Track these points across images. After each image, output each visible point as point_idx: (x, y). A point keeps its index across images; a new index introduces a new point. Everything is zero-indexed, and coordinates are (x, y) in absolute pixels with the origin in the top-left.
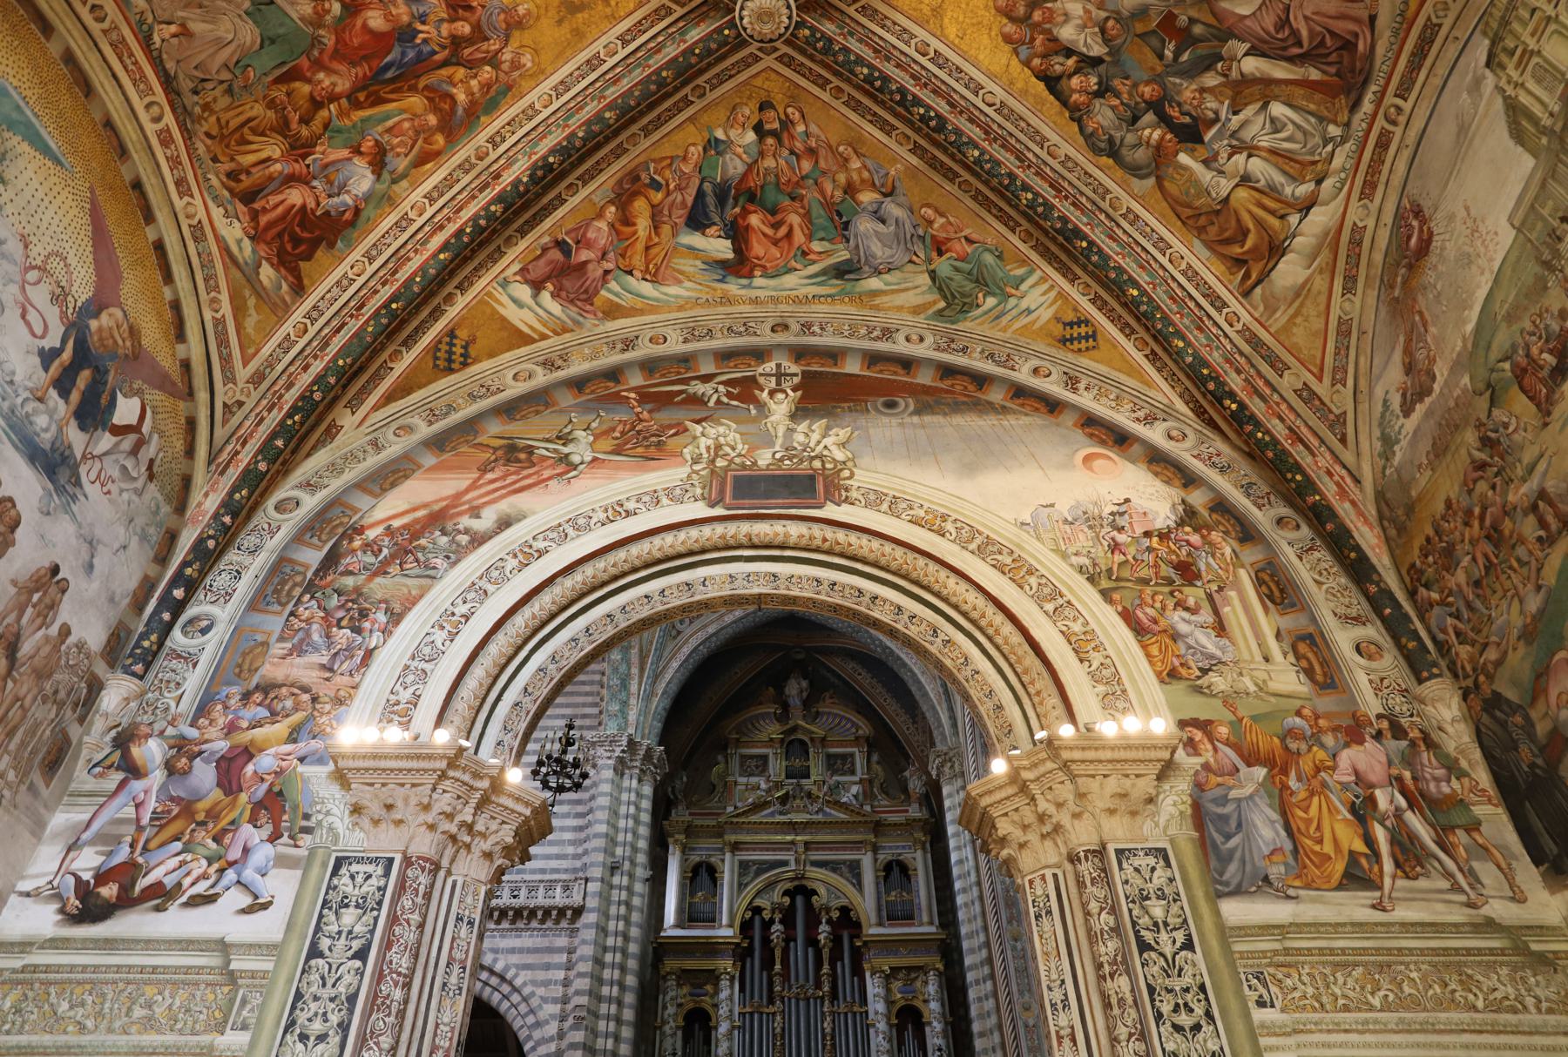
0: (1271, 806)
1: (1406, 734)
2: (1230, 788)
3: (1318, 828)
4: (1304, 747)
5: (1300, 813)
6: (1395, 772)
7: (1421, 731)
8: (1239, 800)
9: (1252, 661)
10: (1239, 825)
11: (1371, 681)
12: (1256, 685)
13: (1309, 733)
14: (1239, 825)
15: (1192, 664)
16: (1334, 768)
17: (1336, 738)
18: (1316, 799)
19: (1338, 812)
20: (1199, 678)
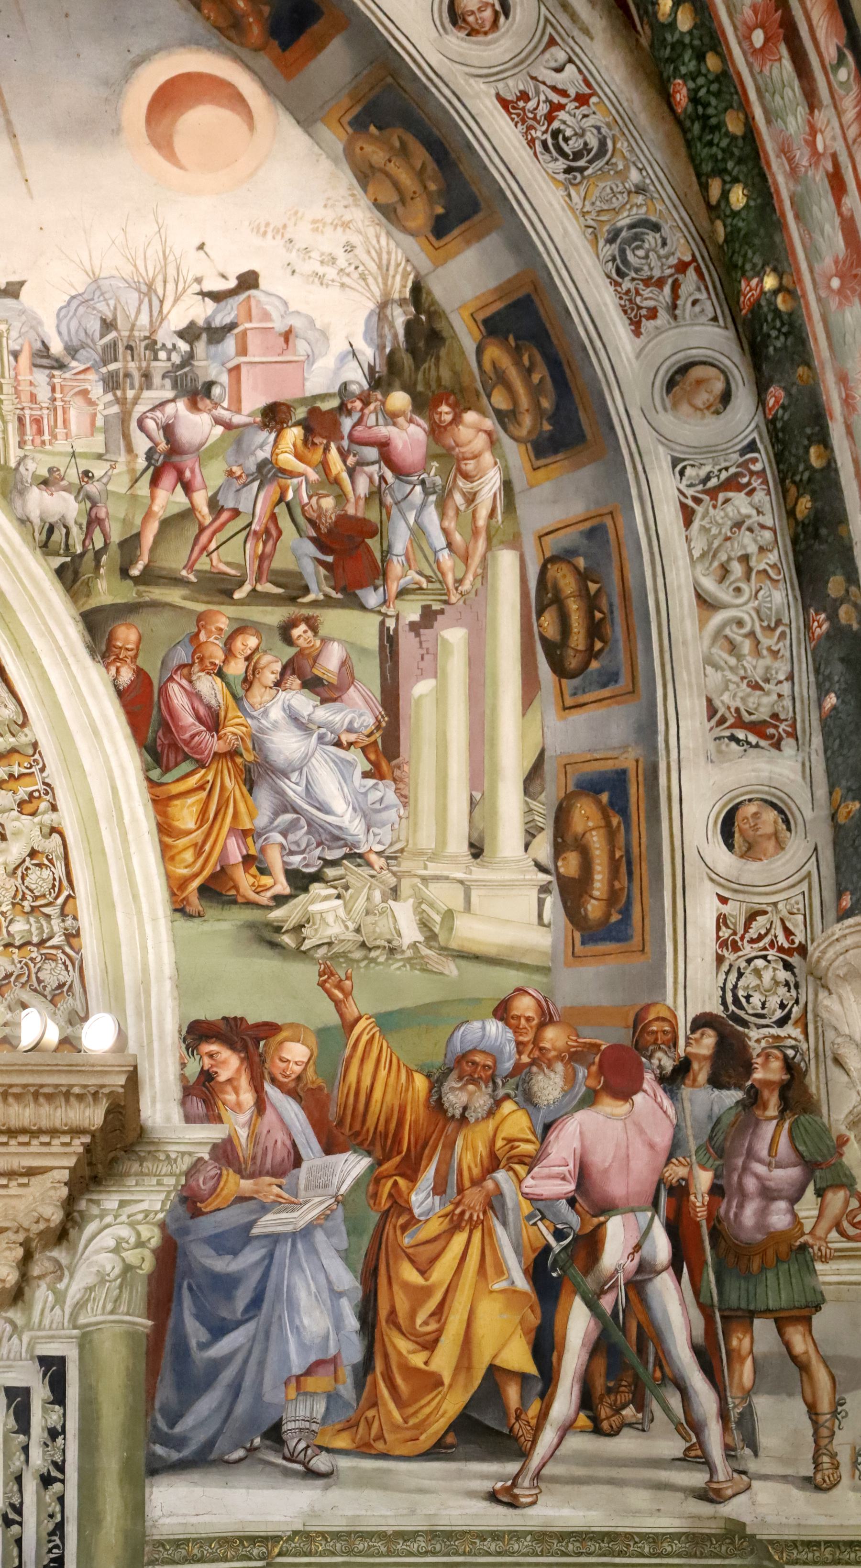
0: (346, 1256)
1: (749, 1068)
2: (265, 1209)
3: (439, 1312)
4: (481, 1100)
5: (409, 1274)
6: (677, 1172)
7: (789, 1066)
8: (275, 1239)
9: (434, 857)
10: (256, 1302)
11: (722, 921)
12: (424, 925)
13: (508, 1066)
14: (256, 1302)
15: (275, 860)
16: (531, 1162)
17: (570, 1079)
18: (459, 1240)
19: (501, 1270)
20: (280, 900)
